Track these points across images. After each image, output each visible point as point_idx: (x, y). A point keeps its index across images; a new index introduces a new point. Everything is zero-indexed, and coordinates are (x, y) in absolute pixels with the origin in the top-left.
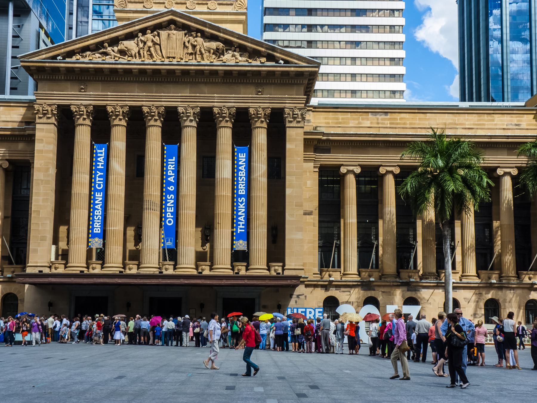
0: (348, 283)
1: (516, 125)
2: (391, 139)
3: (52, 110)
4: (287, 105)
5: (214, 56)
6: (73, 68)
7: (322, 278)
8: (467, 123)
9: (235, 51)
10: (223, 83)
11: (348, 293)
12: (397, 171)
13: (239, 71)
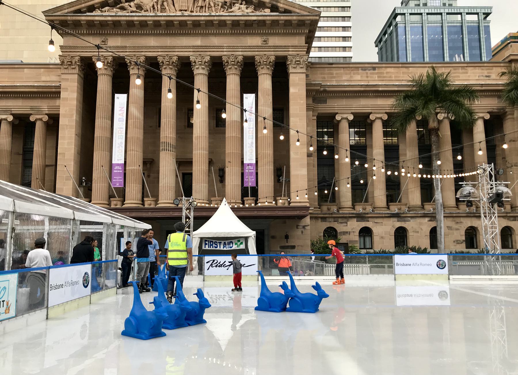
0: (345, 216)
1: (487, 76)
2: (380, 89)
3: (76, 62)
4: (290, 53)
5: (222, 10)
6: (93, 21)
7: (321, 211)
9: (241, 4)
10: (232, 34)
11: (346, 224)
12: (385, 117)
13: (246, 21)
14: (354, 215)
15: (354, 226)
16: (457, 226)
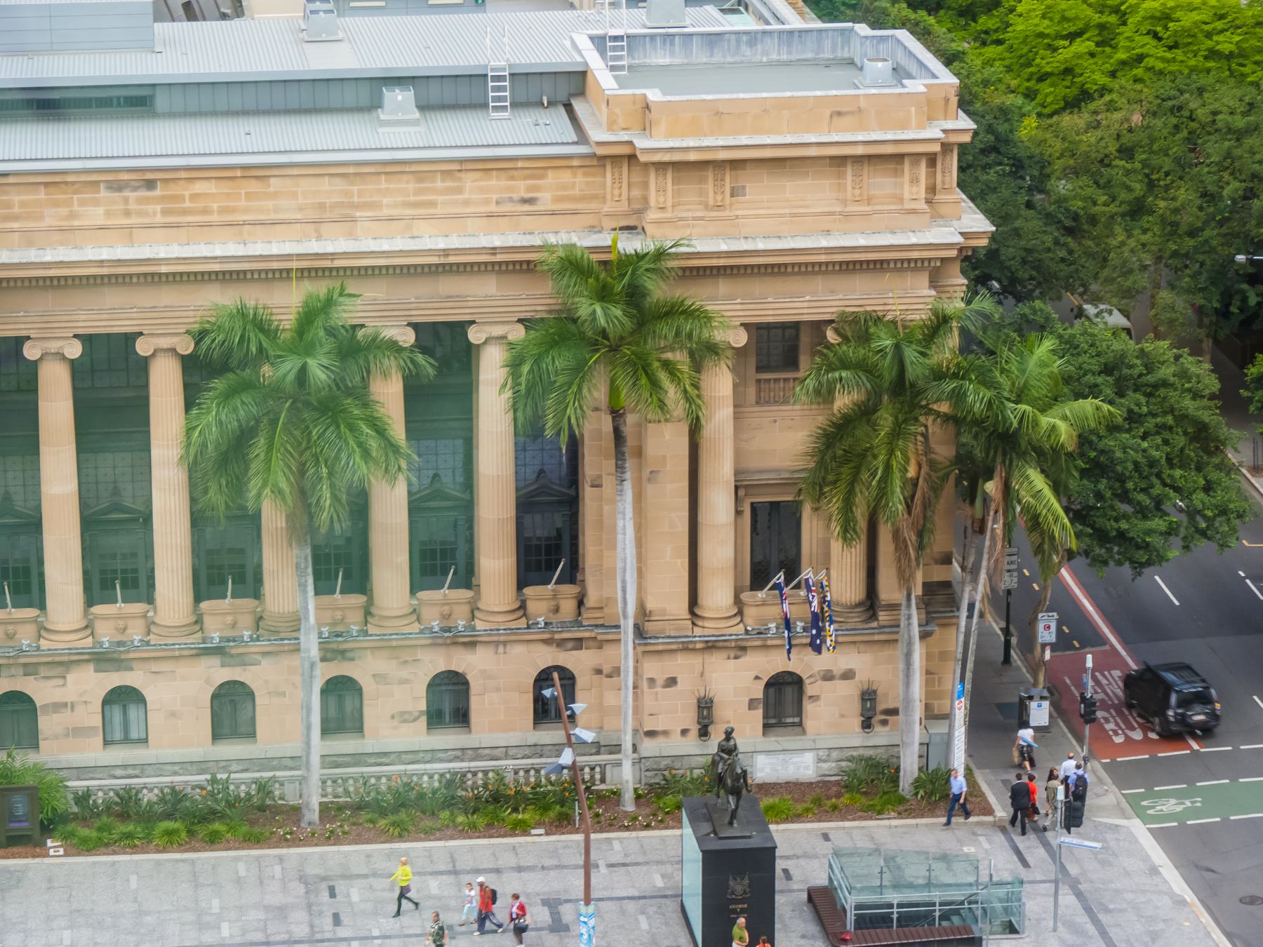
0: (57, 659)
8: (385, 201)
11: (61, 682)
12: (187, 347)
14: (86, 657)
15: (89, 686)
16: (404, 673)
